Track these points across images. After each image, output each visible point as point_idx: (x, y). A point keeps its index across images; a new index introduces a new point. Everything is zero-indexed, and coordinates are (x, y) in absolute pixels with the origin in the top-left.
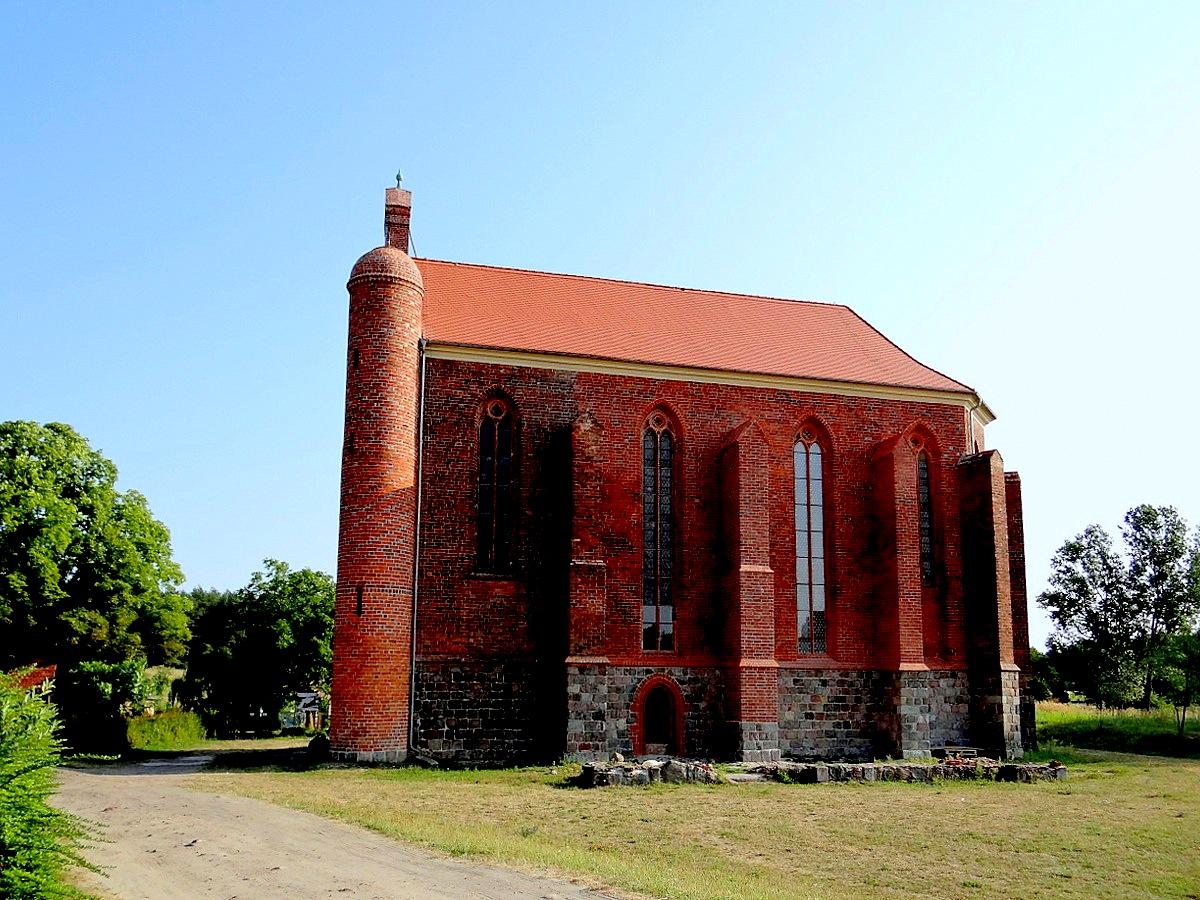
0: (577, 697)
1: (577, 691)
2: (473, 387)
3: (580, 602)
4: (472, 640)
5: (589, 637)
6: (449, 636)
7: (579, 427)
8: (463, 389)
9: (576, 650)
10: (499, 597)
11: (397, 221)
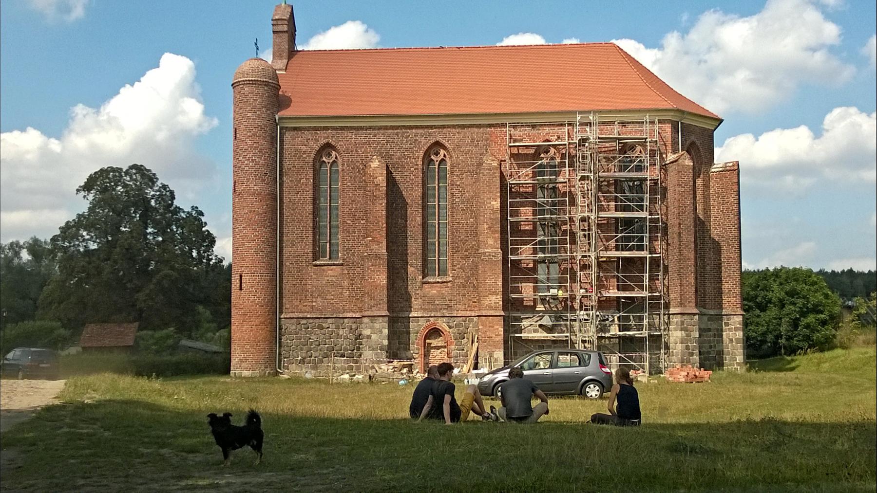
0: (369, 337)
1: (369, 333)
2: (311, 143)
3: (371, 278)
4: (314, 304)
5: (376, 300)
6: (300, 302)
7: (370, 165)
8: (305, 145)
9: (368, 308)
10: (331, 276)
11: (257, 40)
